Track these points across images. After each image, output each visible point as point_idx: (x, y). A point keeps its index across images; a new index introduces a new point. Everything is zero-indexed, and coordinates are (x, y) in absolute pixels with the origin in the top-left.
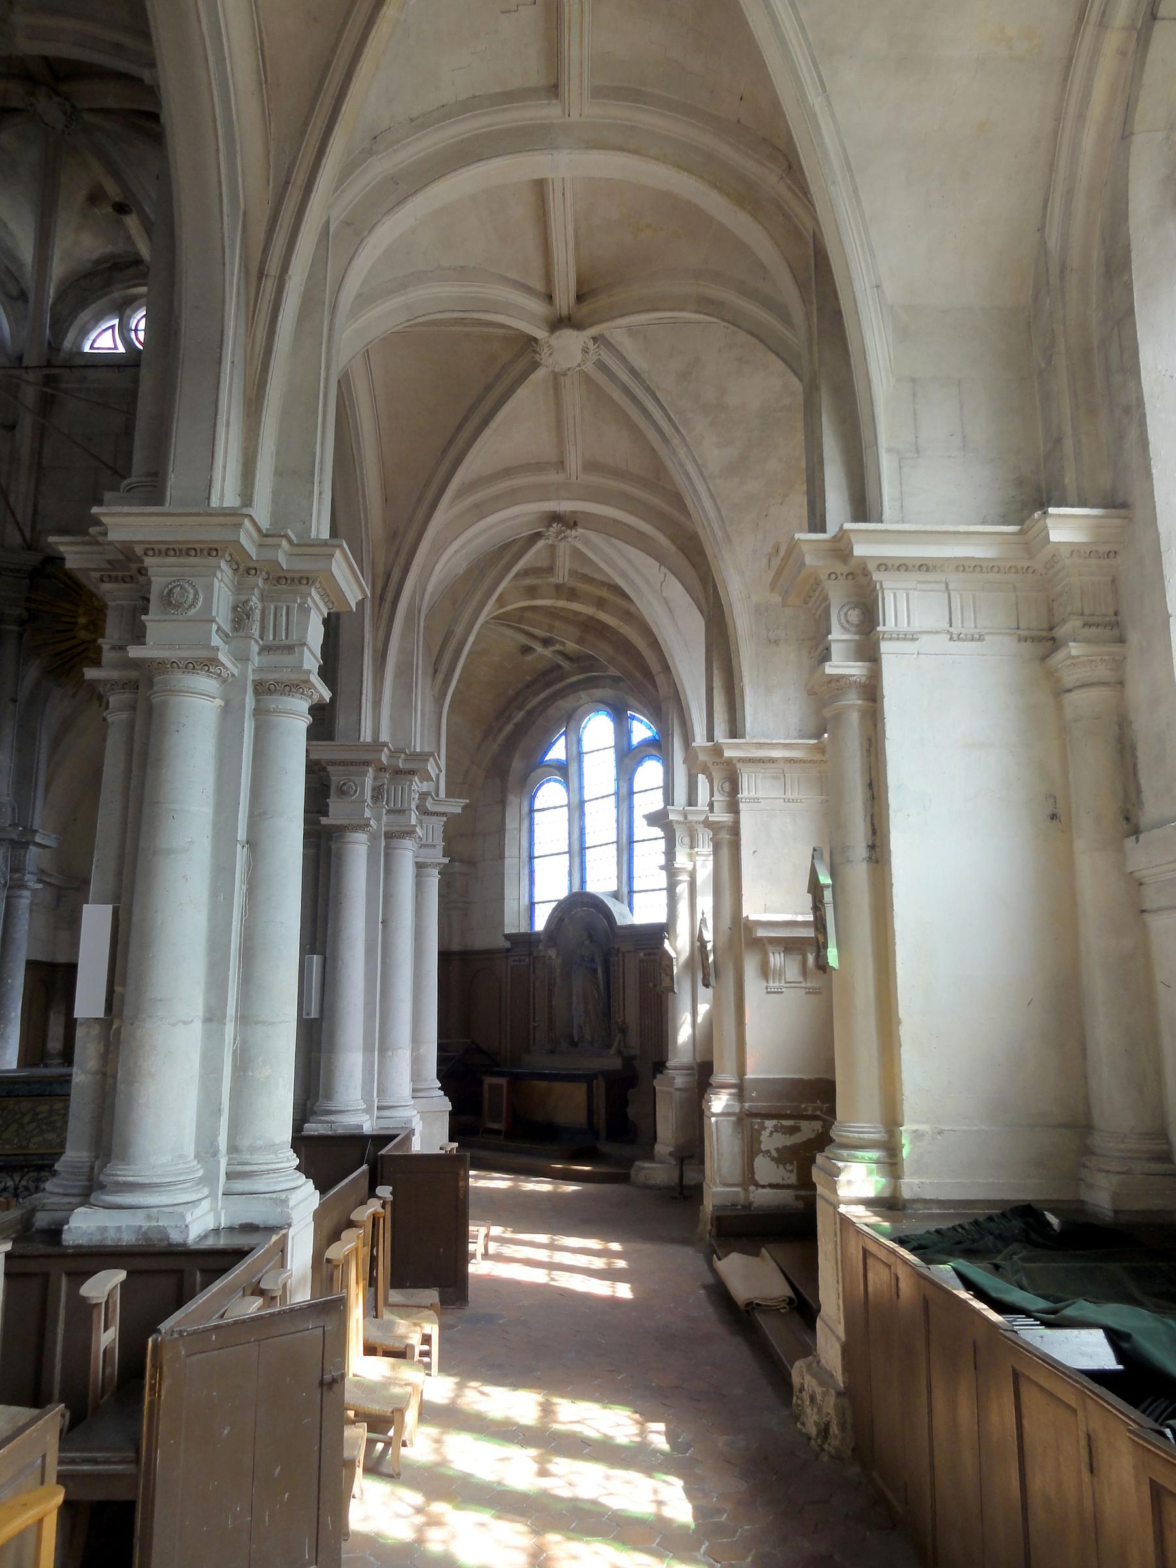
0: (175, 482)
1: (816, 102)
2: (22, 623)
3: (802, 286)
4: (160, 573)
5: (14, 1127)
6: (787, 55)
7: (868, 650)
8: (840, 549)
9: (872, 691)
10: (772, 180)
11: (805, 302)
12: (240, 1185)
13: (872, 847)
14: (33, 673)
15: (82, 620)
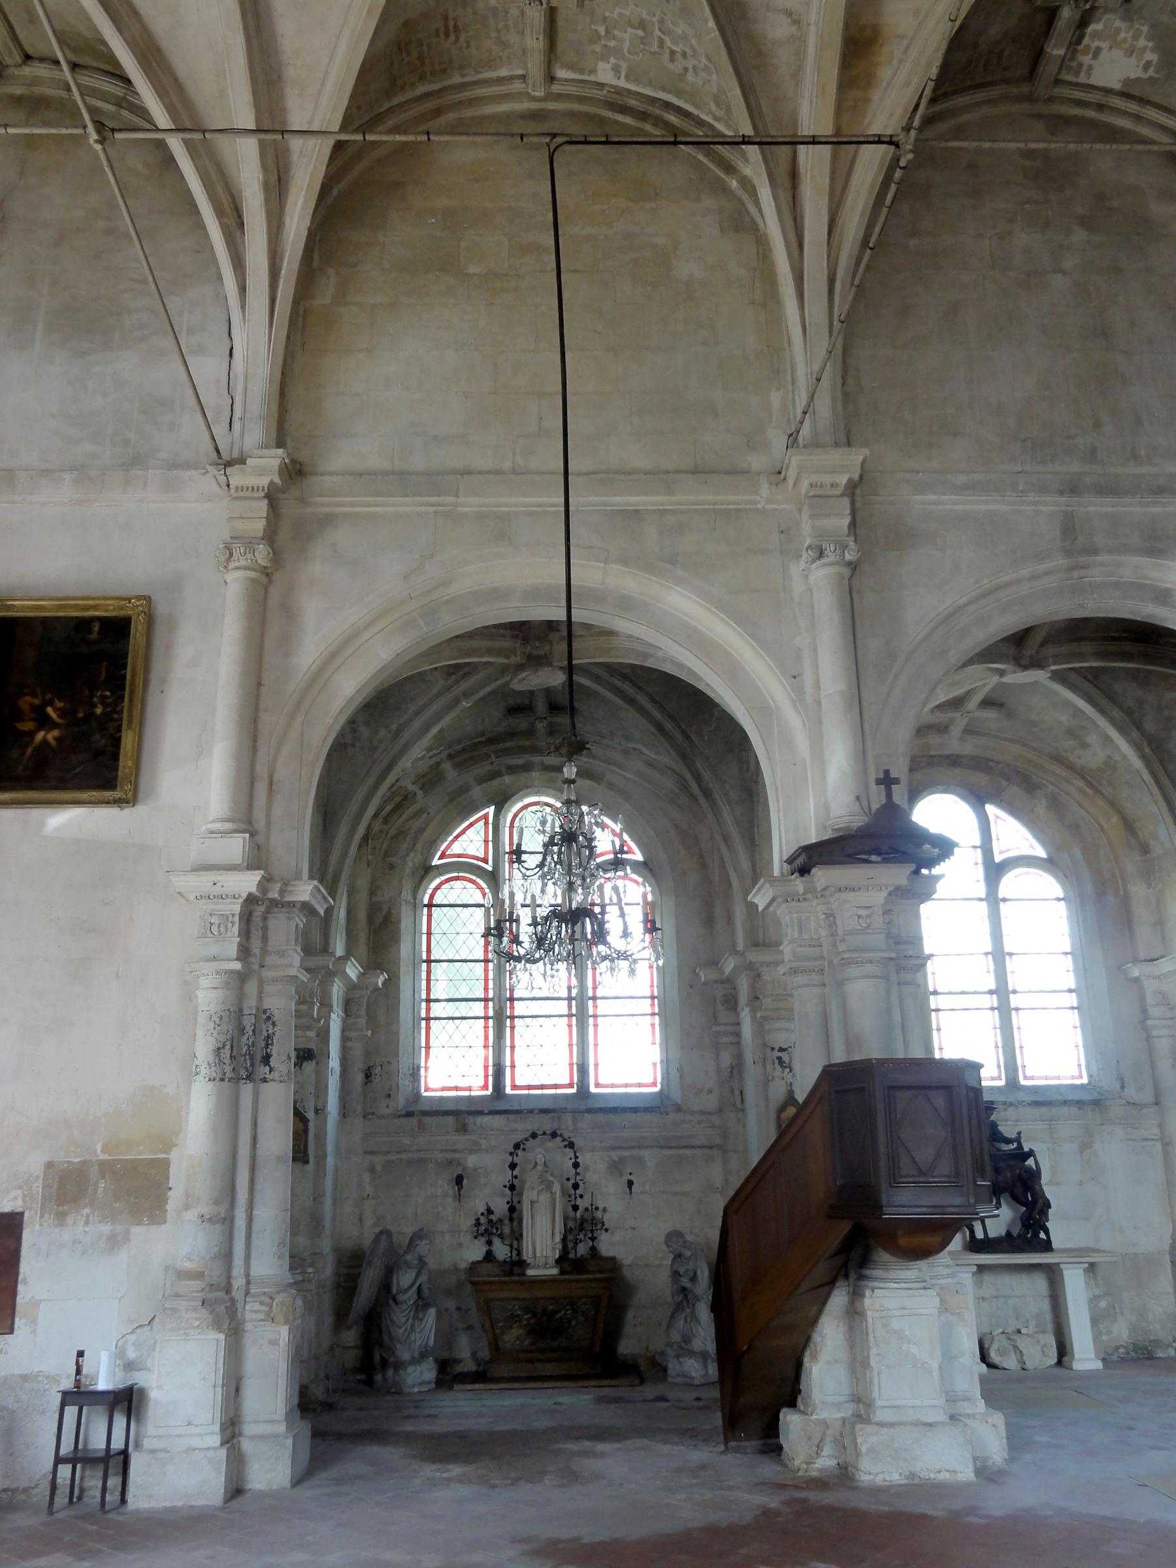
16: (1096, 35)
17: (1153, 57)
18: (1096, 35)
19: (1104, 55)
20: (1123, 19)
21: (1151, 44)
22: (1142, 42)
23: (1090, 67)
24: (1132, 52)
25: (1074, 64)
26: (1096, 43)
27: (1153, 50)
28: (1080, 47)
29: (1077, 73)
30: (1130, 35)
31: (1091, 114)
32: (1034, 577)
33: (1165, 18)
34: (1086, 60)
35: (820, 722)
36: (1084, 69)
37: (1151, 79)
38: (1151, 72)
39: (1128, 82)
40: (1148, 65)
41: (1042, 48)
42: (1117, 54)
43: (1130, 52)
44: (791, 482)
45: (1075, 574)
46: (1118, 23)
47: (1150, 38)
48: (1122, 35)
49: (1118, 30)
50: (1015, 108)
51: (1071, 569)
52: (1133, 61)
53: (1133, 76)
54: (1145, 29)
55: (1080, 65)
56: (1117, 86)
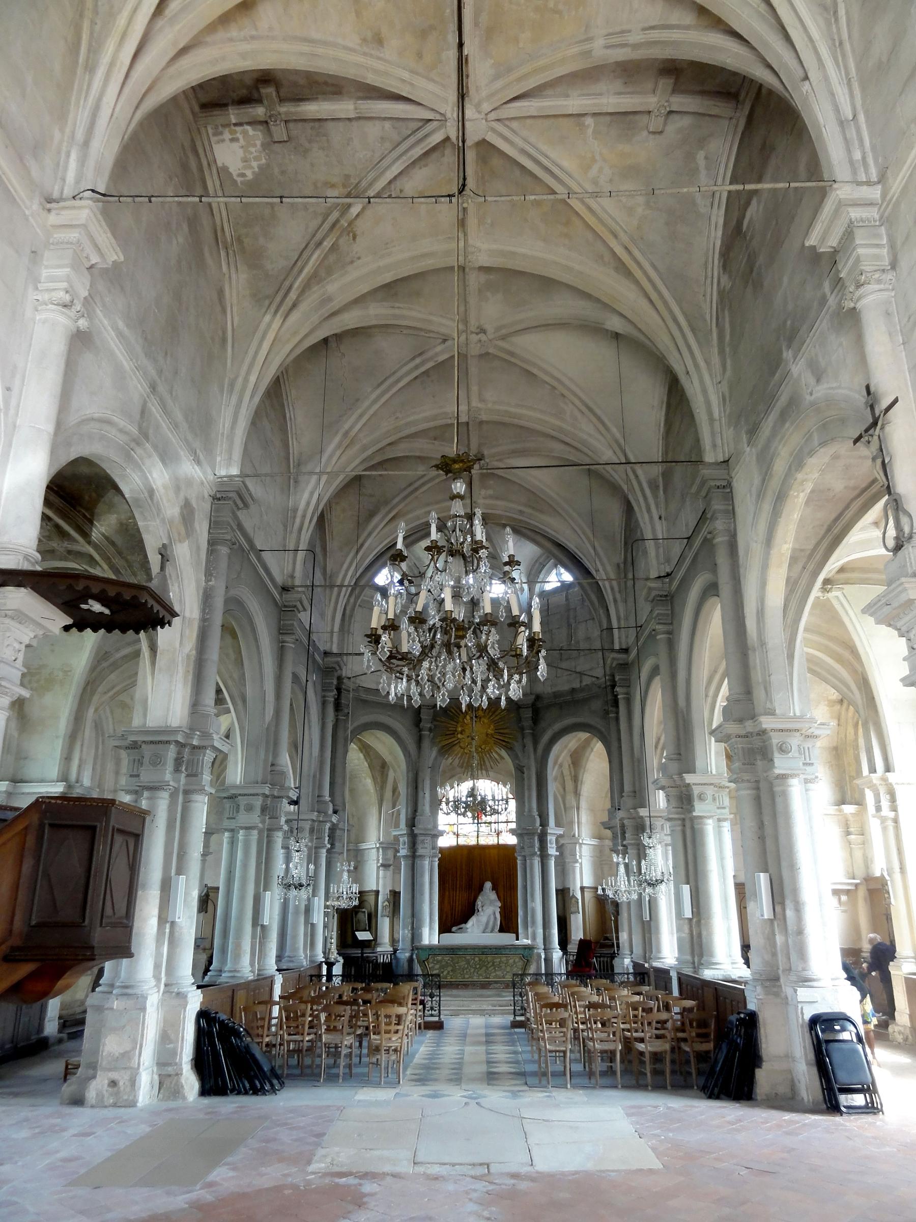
0: (699, 764)
1: (868, 650)
2: (430, 730)
3: (859, 689)
4: (696, 791)
5: (484, 968)
6: (861, 640)
7: (894, 809)
8: (884, 779)
9: (896, 821)
10: (847, 654)
11: (862, 699)
12: (734, 966)
13: (901, 868)
14: (434, 753)
15: (460, 729)
16: (245, 133)
17: (249, 175)
18: (245, 133)
19: (235, 145)
20: (262, 145)
21: (257, 170)
22: (255, 164)
23: (223, 141)
24: (246, 161)
25: (220, 129)
26: (240, 137)
27: (253, 173)
28: (233, 127)
29: (215, 135)
30: (255, 154)
31: (205, 164)
32: (121, 431)
33: (276, 171)
34: (227, 135)
35: (10, 445)
36: (221, 137)
37: (235, 181)
38: (239, 180)
39: (225, 169)
40: (243, 175)
41: (225, 105)
42: (240, 153)
43: (245, 160)
44: (53, 219)
45: (133, 445)
46: (258, 143)
47: (260, 167)
48: (253, 150)
49: (255, 145)
50: (188, 112)
51: (134, 440)
52: (240, 165)
53: (231, 170)
54: (264, 161)
55: (221, 133)
56: (220, 164)
